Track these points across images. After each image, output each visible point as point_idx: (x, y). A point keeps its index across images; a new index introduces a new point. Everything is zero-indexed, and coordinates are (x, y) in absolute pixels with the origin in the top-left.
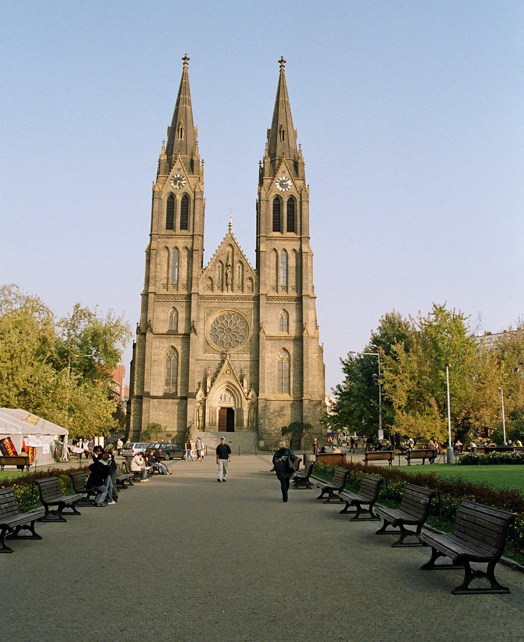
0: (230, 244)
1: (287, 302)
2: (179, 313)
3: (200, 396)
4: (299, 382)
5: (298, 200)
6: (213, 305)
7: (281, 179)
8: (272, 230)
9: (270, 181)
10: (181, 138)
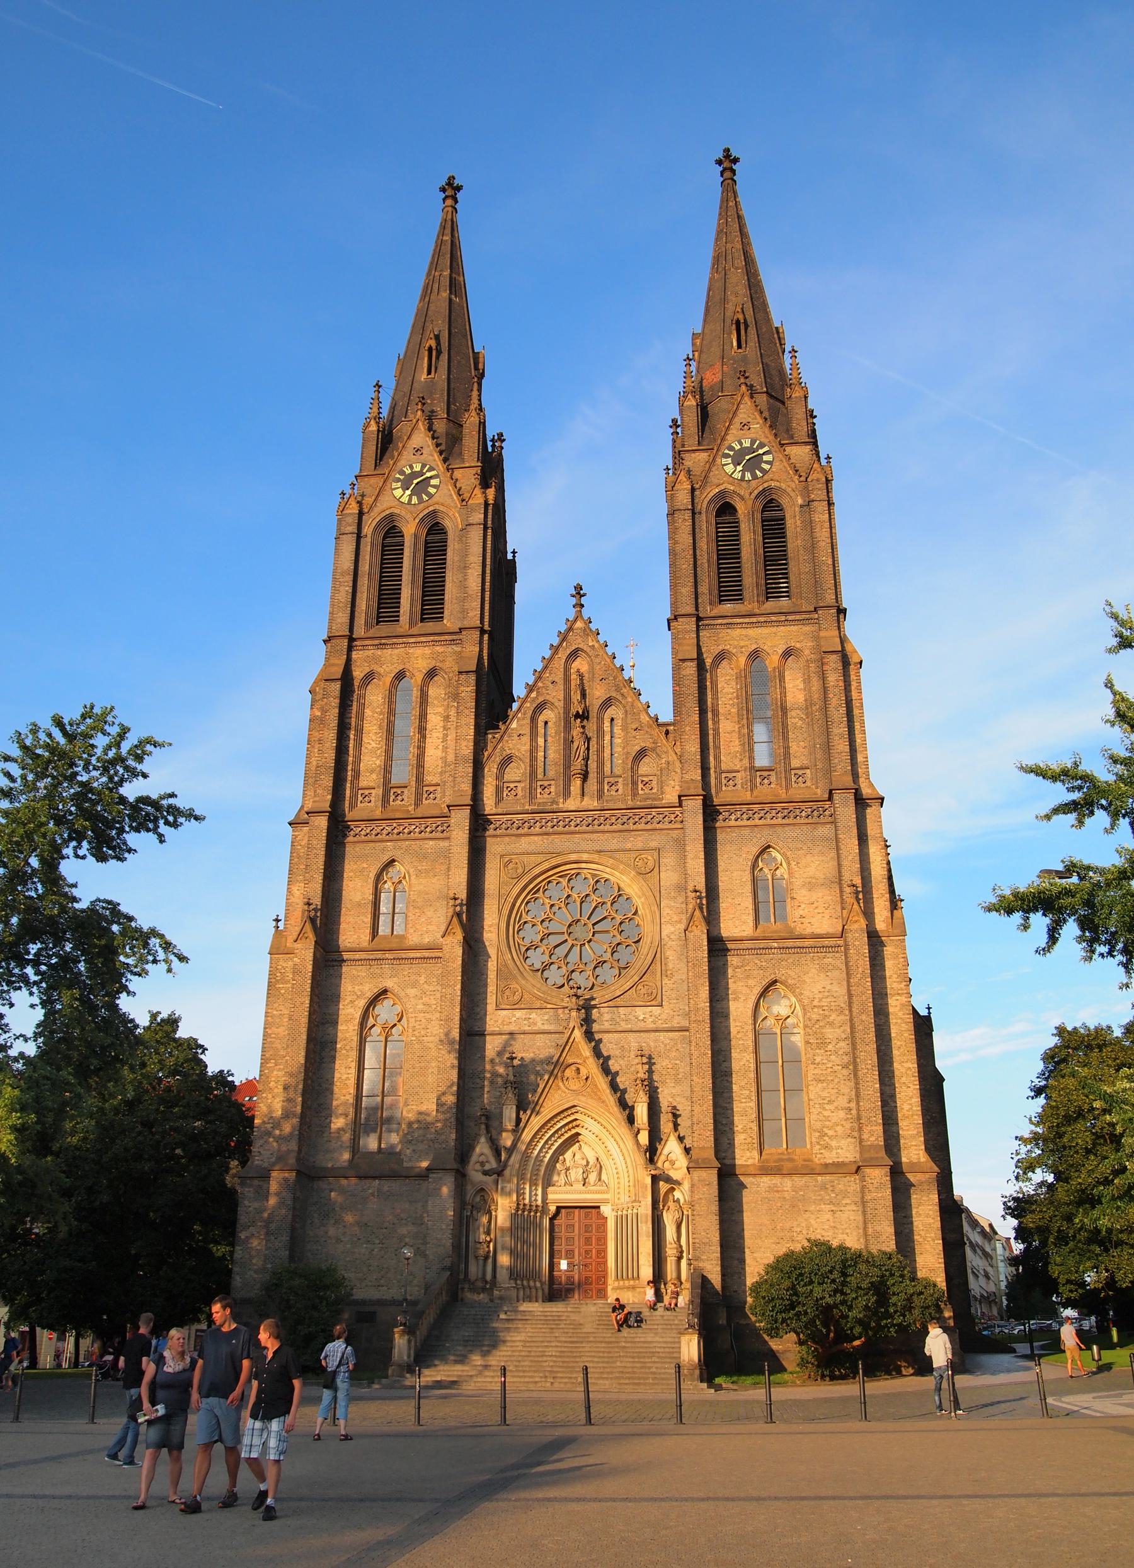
0: (577, 650)
1: (780, 821)
2: (413, 877)
3: (482, 1164)
4: (842, 1101)
5: (800, 501)
6: (524, 844)
7: (738, 447)
8: (717, 600)
9: (703, 456)
10: (429, 373)
